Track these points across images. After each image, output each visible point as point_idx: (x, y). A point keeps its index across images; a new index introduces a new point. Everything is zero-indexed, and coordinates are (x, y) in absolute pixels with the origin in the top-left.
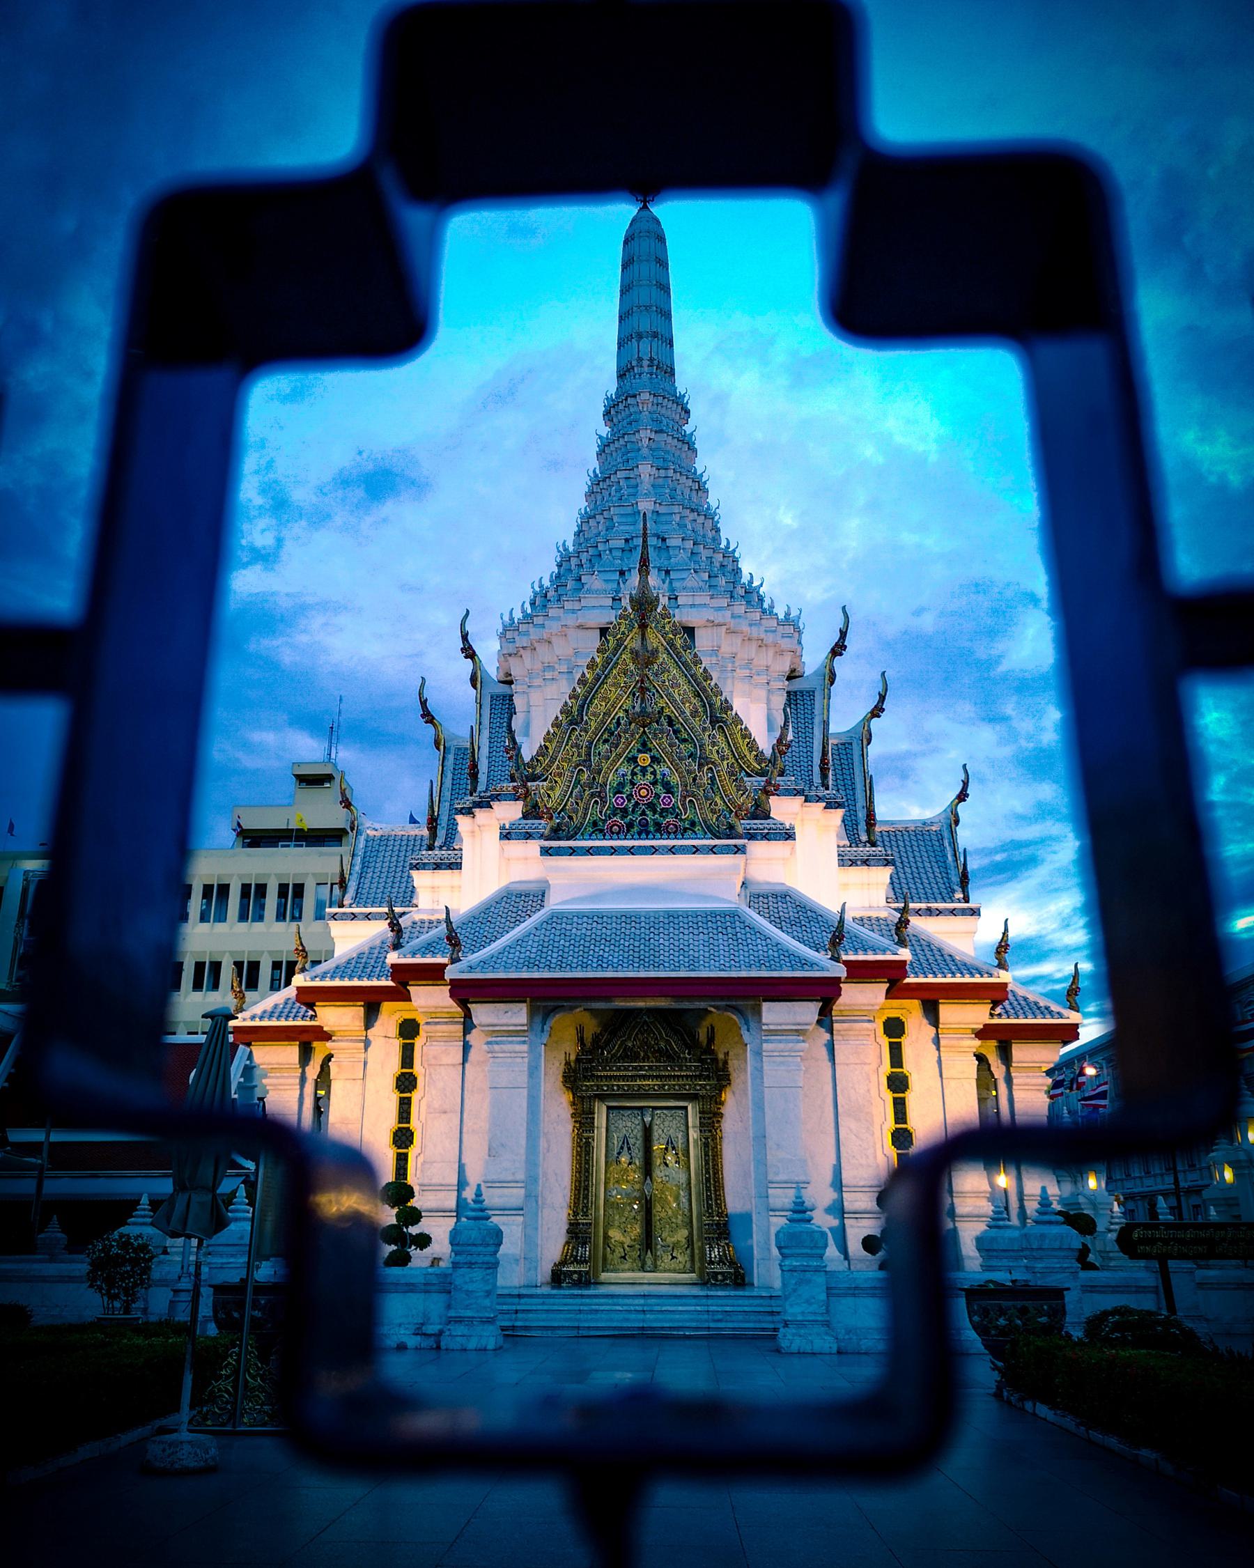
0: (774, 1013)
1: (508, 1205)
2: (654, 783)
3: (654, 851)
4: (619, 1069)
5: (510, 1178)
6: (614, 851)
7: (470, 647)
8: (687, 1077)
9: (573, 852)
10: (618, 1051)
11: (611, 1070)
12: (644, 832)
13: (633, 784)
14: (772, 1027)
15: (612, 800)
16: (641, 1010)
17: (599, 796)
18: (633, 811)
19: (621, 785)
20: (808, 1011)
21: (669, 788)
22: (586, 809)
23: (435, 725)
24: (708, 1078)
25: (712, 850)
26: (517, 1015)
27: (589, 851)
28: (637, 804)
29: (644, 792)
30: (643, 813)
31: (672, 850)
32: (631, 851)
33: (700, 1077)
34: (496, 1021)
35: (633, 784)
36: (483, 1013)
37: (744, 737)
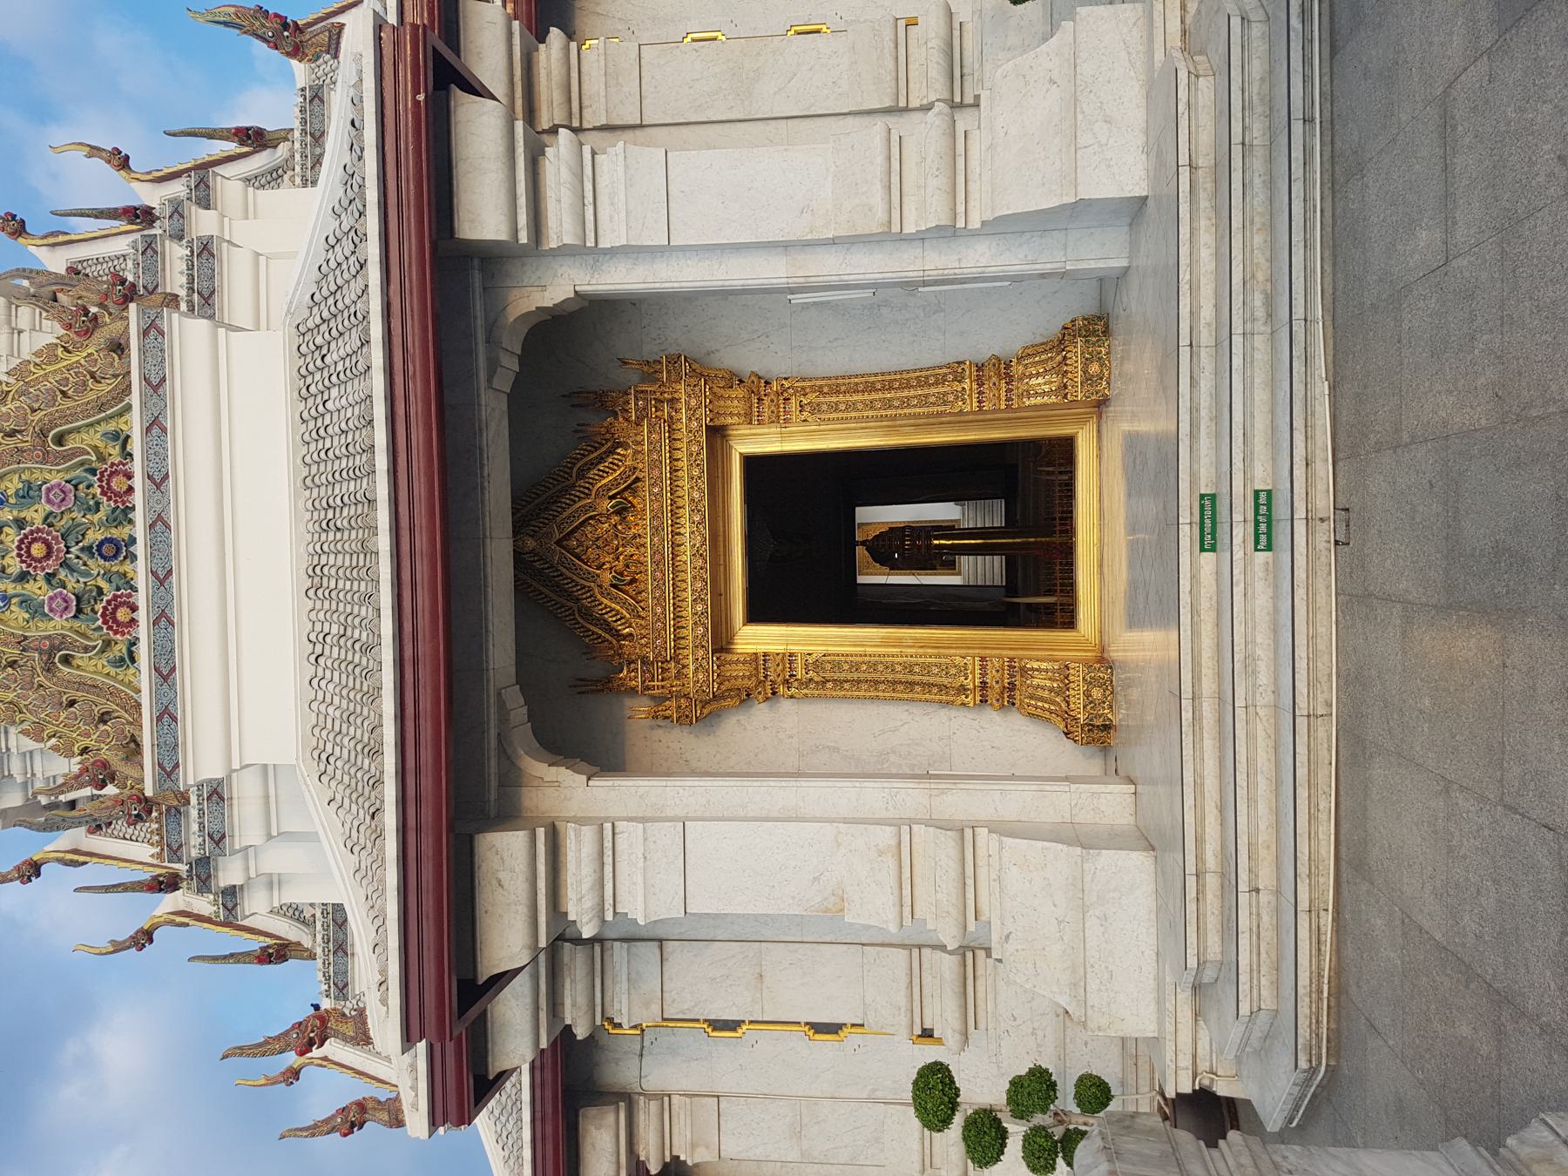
0: (485, 215)
1: (954, 873)
2: (20, 523)
3: (159, 523)
4: (659, 601)
5: (891, 862)
6: (163, 618)
7: (18, 868)
8: (673, 449)
9: (167, 715)
10: (624, 604)
11: (662, 619)
12: (117, 549)
13: (23, 577)
14: (523, 219)
15: (59, 625)
16: (518, 556)
17: (51, 655)
18: (87, 574)
19: (25, 602)
20: (481, 129)
21: (28, 494)
22: (81, 685)
23: (155, 927)
24: (673, 401)
25: (155, 385)
26: (506, 856)
27: (165, 674)
28: (65, 564)
29: (37, 550)
30: (88, 550)
31: (158, 481)
32: (162, 578)
33: (671, 422)
34: (523, 910)
35: (23, 577)
36: (507, 940)
37: (57, 359)
